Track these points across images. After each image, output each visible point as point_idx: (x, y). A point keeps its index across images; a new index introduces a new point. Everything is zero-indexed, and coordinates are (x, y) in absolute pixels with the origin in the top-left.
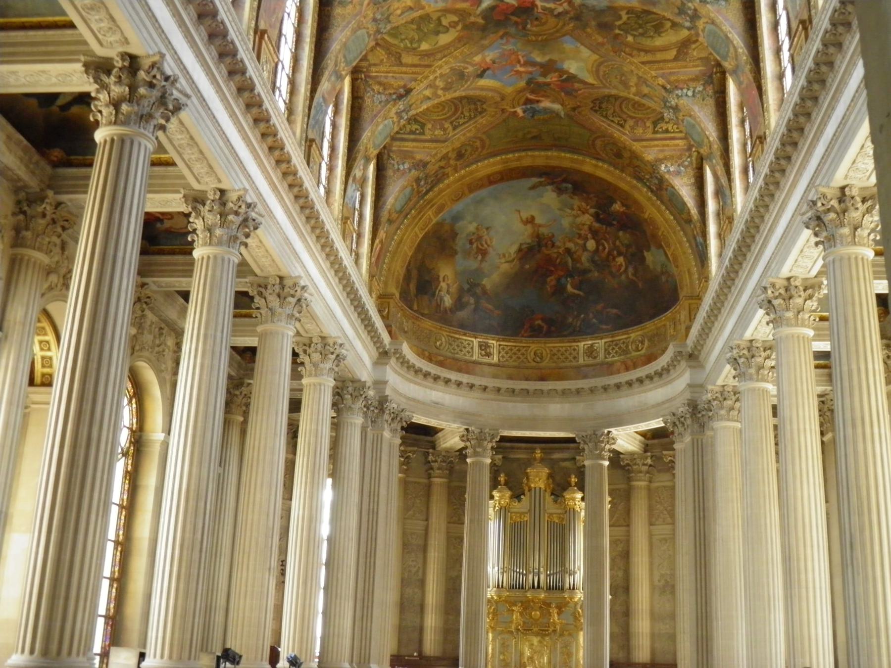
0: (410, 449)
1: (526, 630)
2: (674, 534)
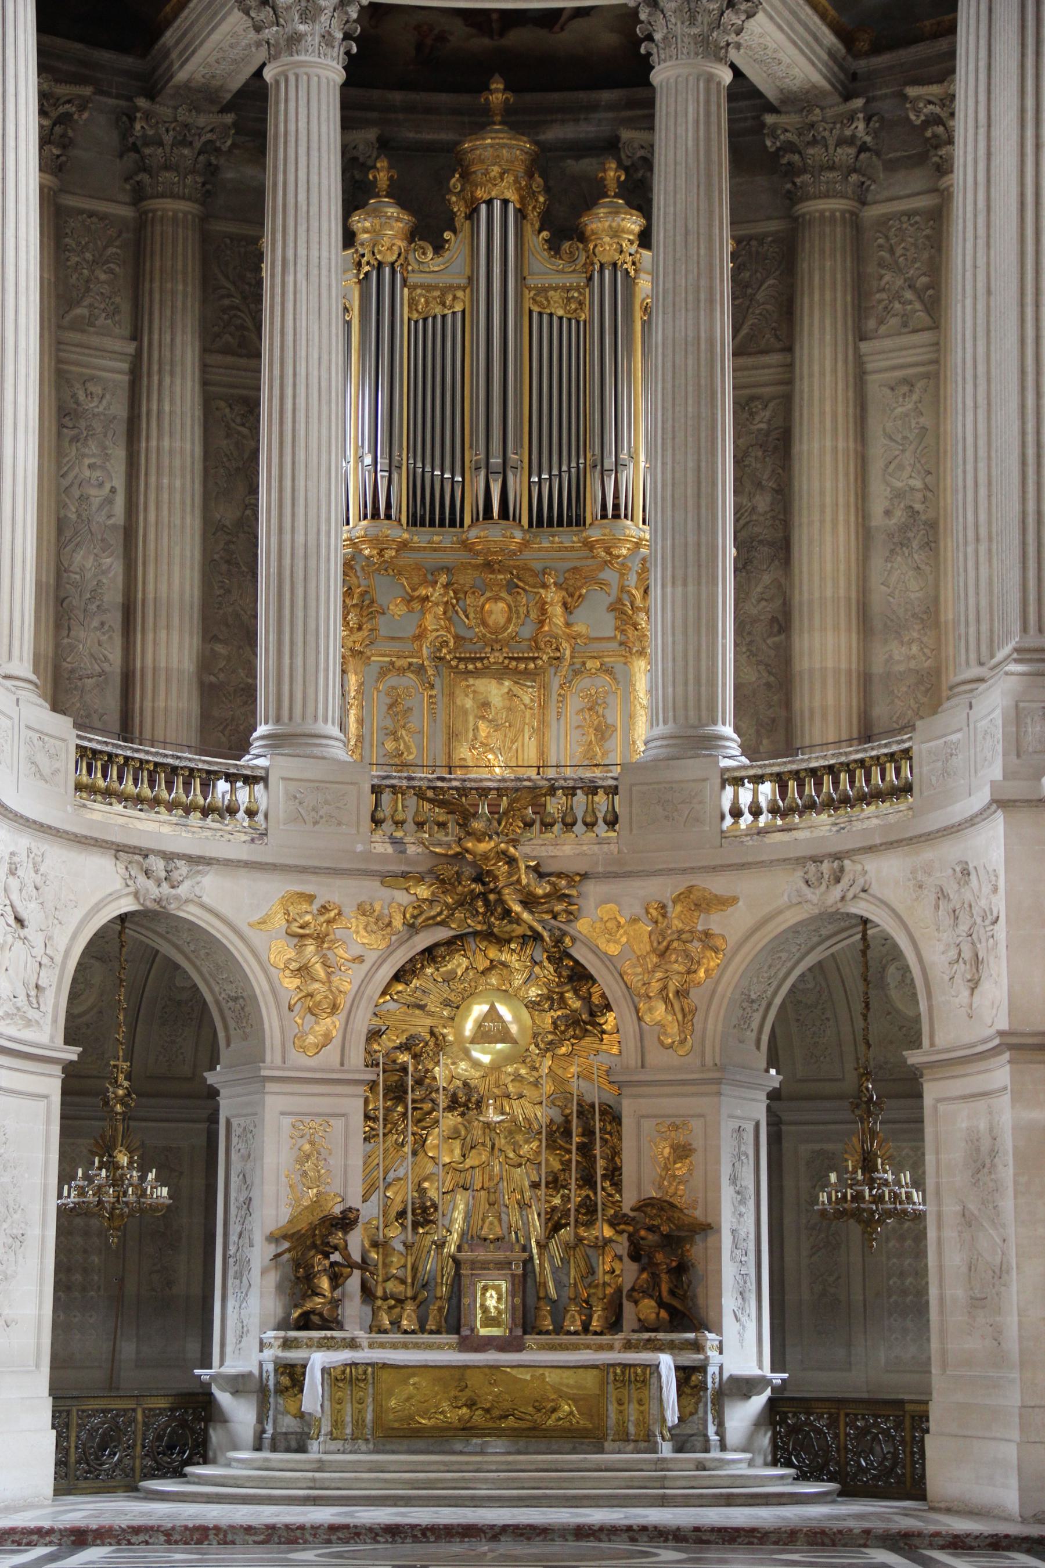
0: (63, 90)
2: (937, 362)
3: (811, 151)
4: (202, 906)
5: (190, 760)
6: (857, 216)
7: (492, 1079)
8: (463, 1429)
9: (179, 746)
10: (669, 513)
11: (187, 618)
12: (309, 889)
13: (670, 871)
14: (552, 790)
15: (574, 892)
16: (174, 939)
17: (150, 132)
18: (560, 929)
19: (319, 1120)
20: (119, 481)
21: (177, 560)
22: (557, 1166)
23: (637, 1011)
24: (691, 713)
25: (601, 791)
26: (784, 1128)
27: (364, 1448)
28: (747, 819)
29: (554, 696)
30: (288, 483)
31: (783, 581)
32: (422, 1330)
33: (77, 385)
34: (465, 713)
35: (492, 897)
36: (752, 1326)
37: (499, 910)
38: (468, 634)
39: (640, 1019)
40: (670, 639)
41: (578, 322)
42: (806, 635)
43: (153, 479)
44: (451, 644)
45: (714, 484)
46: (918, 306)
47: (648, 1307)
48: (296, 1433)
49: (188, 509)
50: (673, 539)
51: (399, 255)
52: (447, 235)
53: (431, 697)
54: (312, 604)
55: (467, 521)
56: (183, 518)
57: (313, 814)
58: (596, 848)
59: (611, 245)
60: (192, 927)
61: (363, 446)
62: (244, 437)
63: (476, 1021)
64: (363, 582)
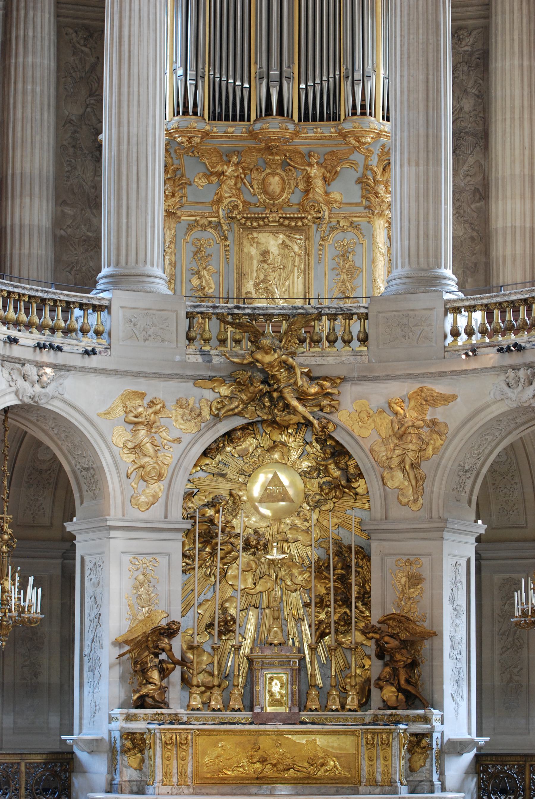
1: (251, 222)
4: (64, 401)
5: (54, 293)
7: (275, 528)
8: (257, 778)
9: (38, 282)
10: (406, 113)
11: (45, 188)
12: (141, 389)
13: (408, 377)
14: (319, 316)
15: (335, 391)
16: (43, 425)
18: (325, 418)
19: (149, 558)
21: (37, 145)
22: (323, 591)
23: (383, 479)
24: (422, 260)
25: (355, 317)
26: (483, 562)
27: (186, 791)
28: (464, 337)
30: (125, 90)
31: (483, 163)
32: (226, 707)
34: (251, 257)
35: (275, 395)
36: (464, 704)
37: (281, 404)
38: (253, 200)
39: (384, 484)
40: (406, 205)
42: (500, 202)
43: (20, 86)
44: (241, 207)
45: (438, 91)
47: (390, 692)
48: (137, 781)
49: (46, 107)
50: (409, 132)
53: (226, 246)
54: (143, 178)
55: (253, 117)
56: (42, 114)
58: (352, 358)
60: (57, 417)
61: (176, 62)
62: (86, 54)
63: (263, 485)
64: (176, 162)
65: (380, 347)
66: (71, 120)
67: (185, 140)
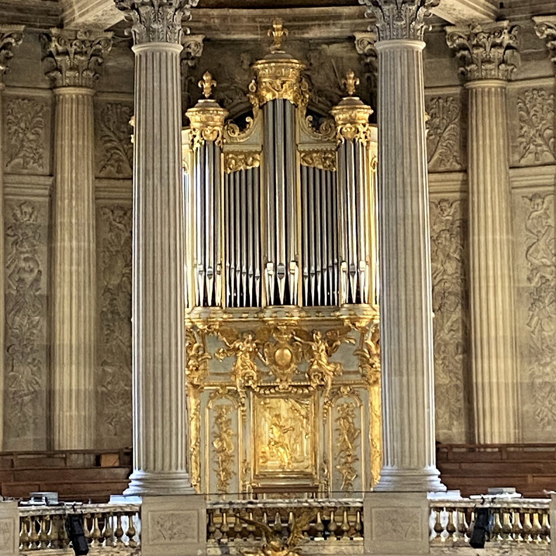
3: (475, 51)
6: (505, 88)
17: (60, 48)
20: (43, 267)
29: (321, 410)
33: (16, 208)
38: (265, 370)
41: (331, 173)
44: (255, 378)
46: (545, 148)
51: (218, 136)
52: (248, 119)
53: (243, 411)
54: (167, 392)
55: (264, 303)
57: (170, 532)
59: (351, 128)
62: (120, 230)
65: (374, 539)
66: (109, 289)
67: (206, 327)
